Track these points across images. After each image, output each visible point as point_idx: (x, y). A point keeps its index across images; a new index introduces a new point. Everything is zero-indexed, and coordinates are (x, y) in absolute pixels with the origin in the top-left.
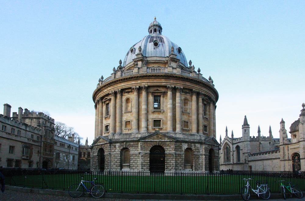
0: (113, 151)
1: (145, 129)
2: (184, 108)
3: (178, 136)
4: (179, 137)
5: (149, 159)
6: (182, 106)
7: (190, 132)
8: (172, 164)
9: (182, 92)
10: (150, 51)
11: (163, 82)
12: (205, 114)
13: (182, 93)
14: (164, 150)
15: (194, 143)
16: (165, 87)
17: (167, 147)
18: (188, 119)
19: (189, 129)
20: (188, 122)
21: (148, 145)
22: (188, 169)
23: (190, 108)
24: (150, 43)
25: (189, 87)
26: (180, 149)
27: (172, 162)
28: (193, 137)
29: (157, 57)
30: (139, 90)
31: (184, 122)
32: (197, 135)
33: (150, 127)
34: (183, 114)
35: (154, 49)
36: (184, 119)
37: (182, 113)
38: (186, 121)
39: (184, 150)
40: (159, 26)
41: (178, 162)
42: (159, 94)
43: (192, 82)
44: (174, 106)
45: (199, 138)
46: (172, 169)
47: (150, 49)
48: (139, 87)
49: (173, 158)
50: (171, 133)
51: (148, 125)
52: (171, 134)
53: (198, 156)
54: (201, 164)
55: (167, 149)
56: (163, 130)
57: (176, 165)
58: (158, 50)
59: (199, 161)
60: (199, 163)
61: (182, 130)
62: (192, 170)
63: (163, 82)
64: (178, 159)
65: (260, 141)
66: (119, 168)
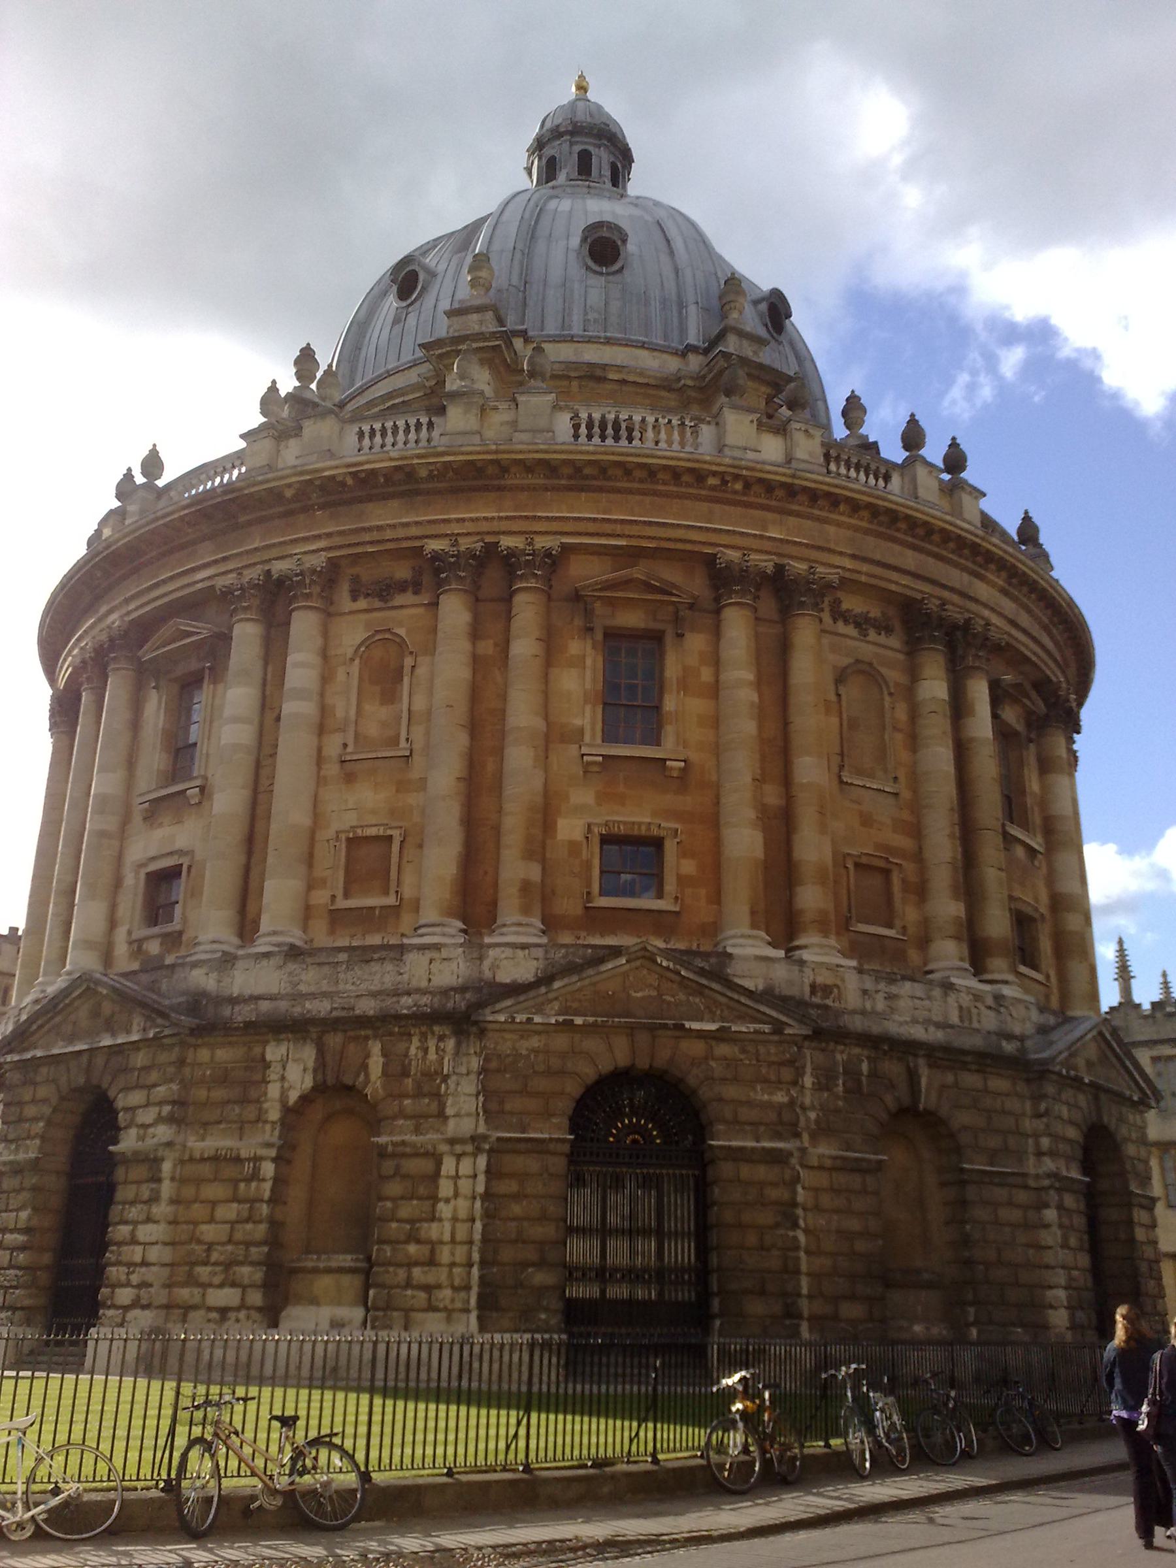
4: (247, 992)
6: (340, 713)
7: (407, 921)
9: (354, 599)
13: (347, 604)
15: (387, 1024)
17: (136, 1098)
18: (392, 812)
19: (391, 900)
20: (390, 838)
23: (419, 704)
26: (244, 1101)
28: (382, 976)
29: (389, 374)
31: (354, 842)
32: (437, 947)
34: (350, 778)
36: (351, 819)
37: (332, 769)
38: (372, 832)
39: (274, 1115)
40: (572, 133)
41: (209, 1232)
42: (194, 665)
43: (418, 493)
46: (136, 1304)
51: (112, 924)
53: (427, 1166)
54: (445, 1255)
55: (128, 1116)
57: (183, 1270)
58: (412, 320)
59: (433, 1218)
60: (434, 1245)
64: (214, 1204)
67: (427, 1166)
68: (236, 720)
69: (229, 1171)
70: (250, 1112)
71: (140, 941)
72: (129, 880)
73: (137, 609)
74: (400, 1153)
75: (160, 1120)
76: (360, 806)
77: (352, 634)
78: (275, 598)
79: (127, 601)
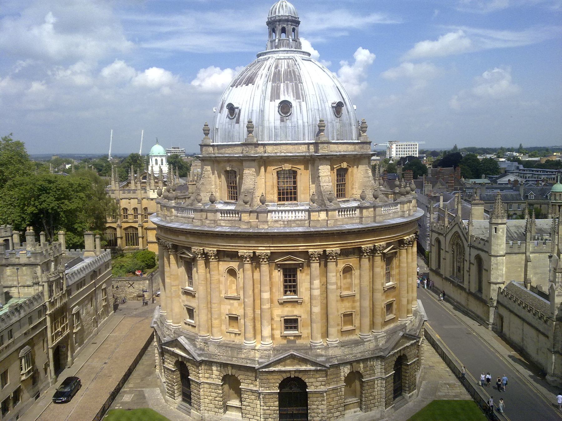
0: (207, 375)
1: (269, 341)
2: (344, 284)
3: (331, 352)
5: (277, 403)
6: (339, 285)
8: (320, 411)
10: (272, 124)
11: (301, 247)
12: (388, 276)
14: (305, 386)
16: (305, 254)
17: (312, 380)
21: (276, 377)
22: (353, 410)
24: (271, 101)
25: (353, 244)
27: (320, 407)
28: (361, 348)
30: (255, 260)
33: (277, 334)
34: (342, 301)
35: (282, 121)
39: (343, 378)
41: (332, 403)
44: (324, 287)
45: (372, 346)
47: (272, 120)
48: (254, 253)
49: (324, 400)
50: (318, 349)
51: (272, 329)
52: (318, 350)
54: (376, 397)
55: (310, 384)
56: (303, 339)
58: (289, 123)
59: (374, 391)
61: (340, 334)
62: (359, 409)
63: (301, 247)
65: (528, 254)
66: (222, 411)
67: (373, 383)
68: (318, 289)
69: (335, 391)
70: (338, 379)
71: (286, 336)
72: (277, 319)
73: (273, 250)
74: (368, 382)
75: (321, 385)
76: (346, 307)
77: (342, 265)
78: (324, 258)
79: (270, 247)
